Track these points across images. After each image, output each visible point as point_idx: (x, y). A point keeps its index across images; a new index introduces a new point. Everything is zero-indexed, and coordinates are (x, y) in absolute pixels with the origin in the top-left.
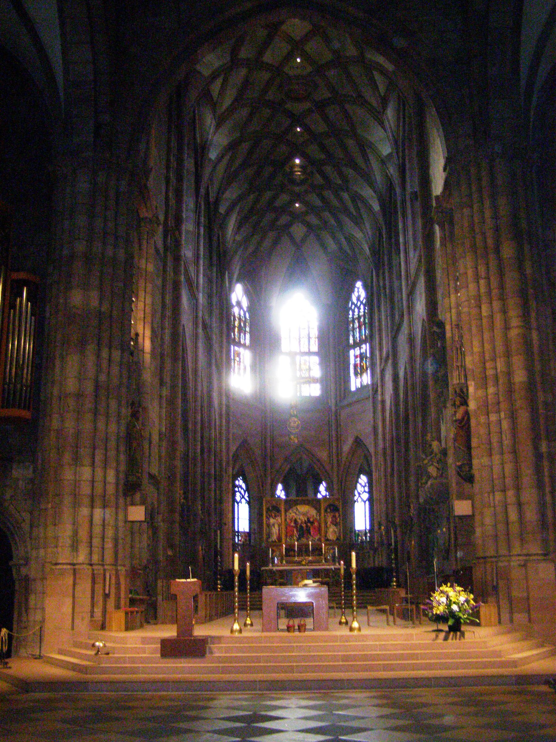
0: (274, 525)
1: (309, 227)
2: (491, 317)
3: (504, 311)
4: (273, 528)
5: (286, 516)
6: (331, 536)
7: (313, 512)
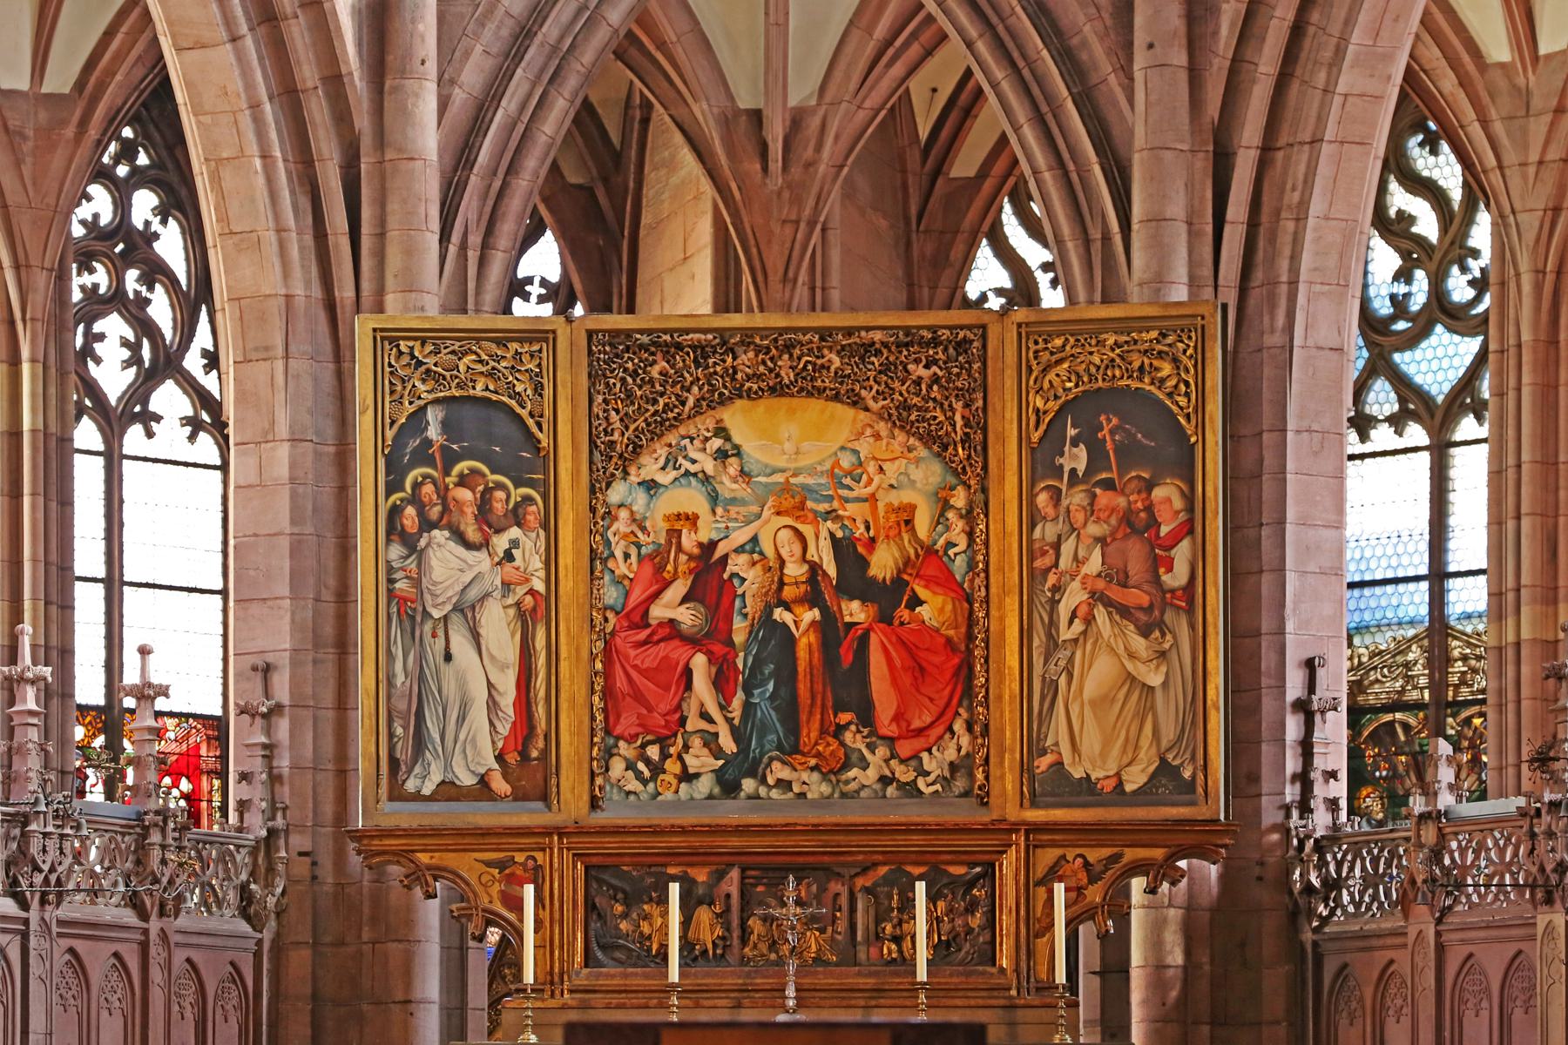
0: (467, 610)
4: (460, 643)
5: (599, 514)
6: (1091, 741)
7: (914, 477)
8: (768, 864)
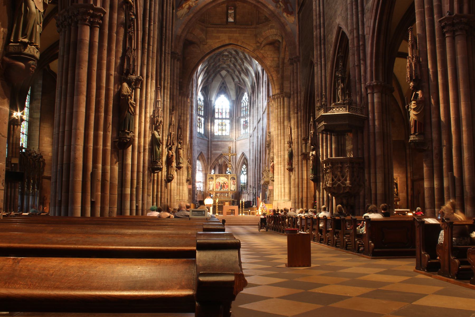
1: (228, 72)
2: (281, 140)
3: (284, 139)
7: (226, 180)
8: (221, 193)
